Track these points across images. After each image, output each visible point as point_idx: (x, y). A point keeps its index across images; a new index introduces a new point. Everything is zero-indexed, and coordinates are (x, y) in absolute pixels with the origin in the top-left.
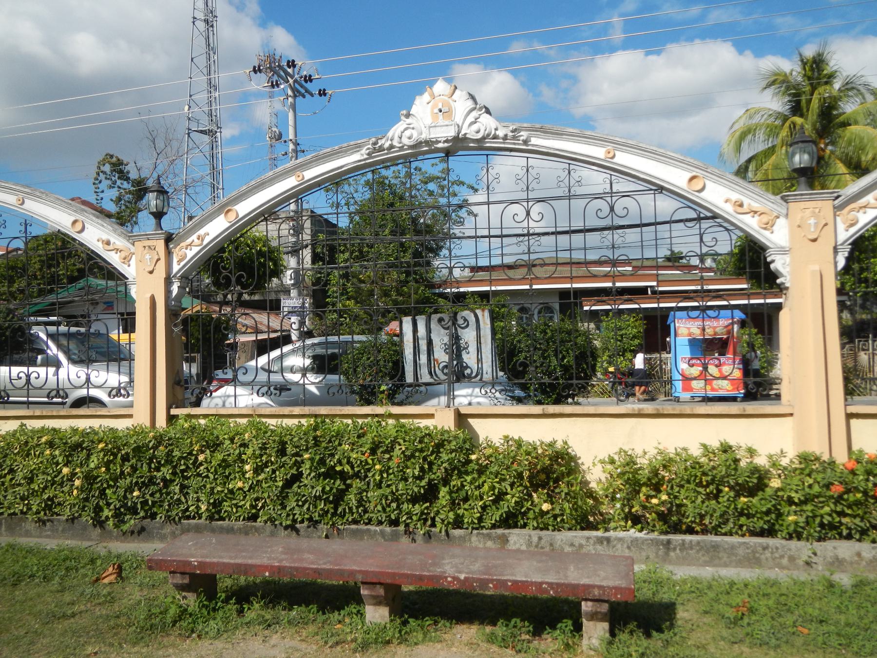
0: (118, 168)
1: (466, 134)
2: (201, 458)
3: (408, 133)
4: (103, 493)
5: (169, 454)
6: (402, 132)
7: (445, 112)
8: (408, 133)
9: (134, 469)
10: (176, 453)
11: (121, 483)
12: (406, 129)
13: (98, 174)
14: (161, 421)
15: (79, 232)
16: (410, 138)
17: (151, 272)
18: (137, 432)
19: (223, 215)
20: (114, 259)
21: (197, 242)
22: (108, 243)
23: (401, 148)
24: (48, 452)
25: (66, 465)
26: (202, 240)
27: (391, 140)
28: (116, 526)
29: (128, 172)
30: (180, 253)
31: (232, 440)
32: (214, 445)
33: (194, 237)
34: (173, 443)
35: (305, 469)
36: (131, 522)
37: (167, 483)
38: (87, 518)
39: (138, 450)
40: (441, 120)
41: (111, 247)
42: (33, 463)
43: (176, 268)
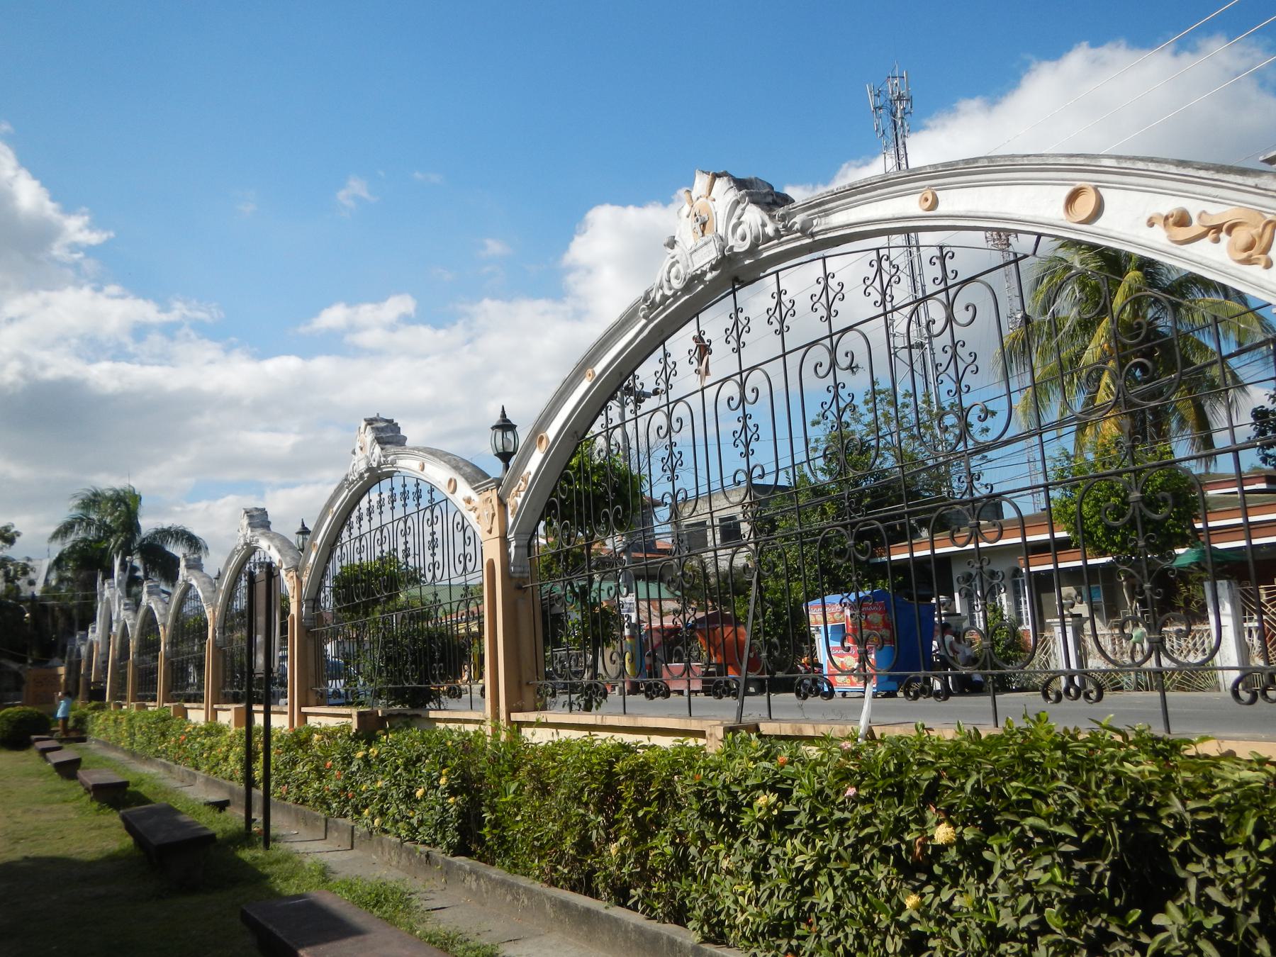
41: (1196, 228)
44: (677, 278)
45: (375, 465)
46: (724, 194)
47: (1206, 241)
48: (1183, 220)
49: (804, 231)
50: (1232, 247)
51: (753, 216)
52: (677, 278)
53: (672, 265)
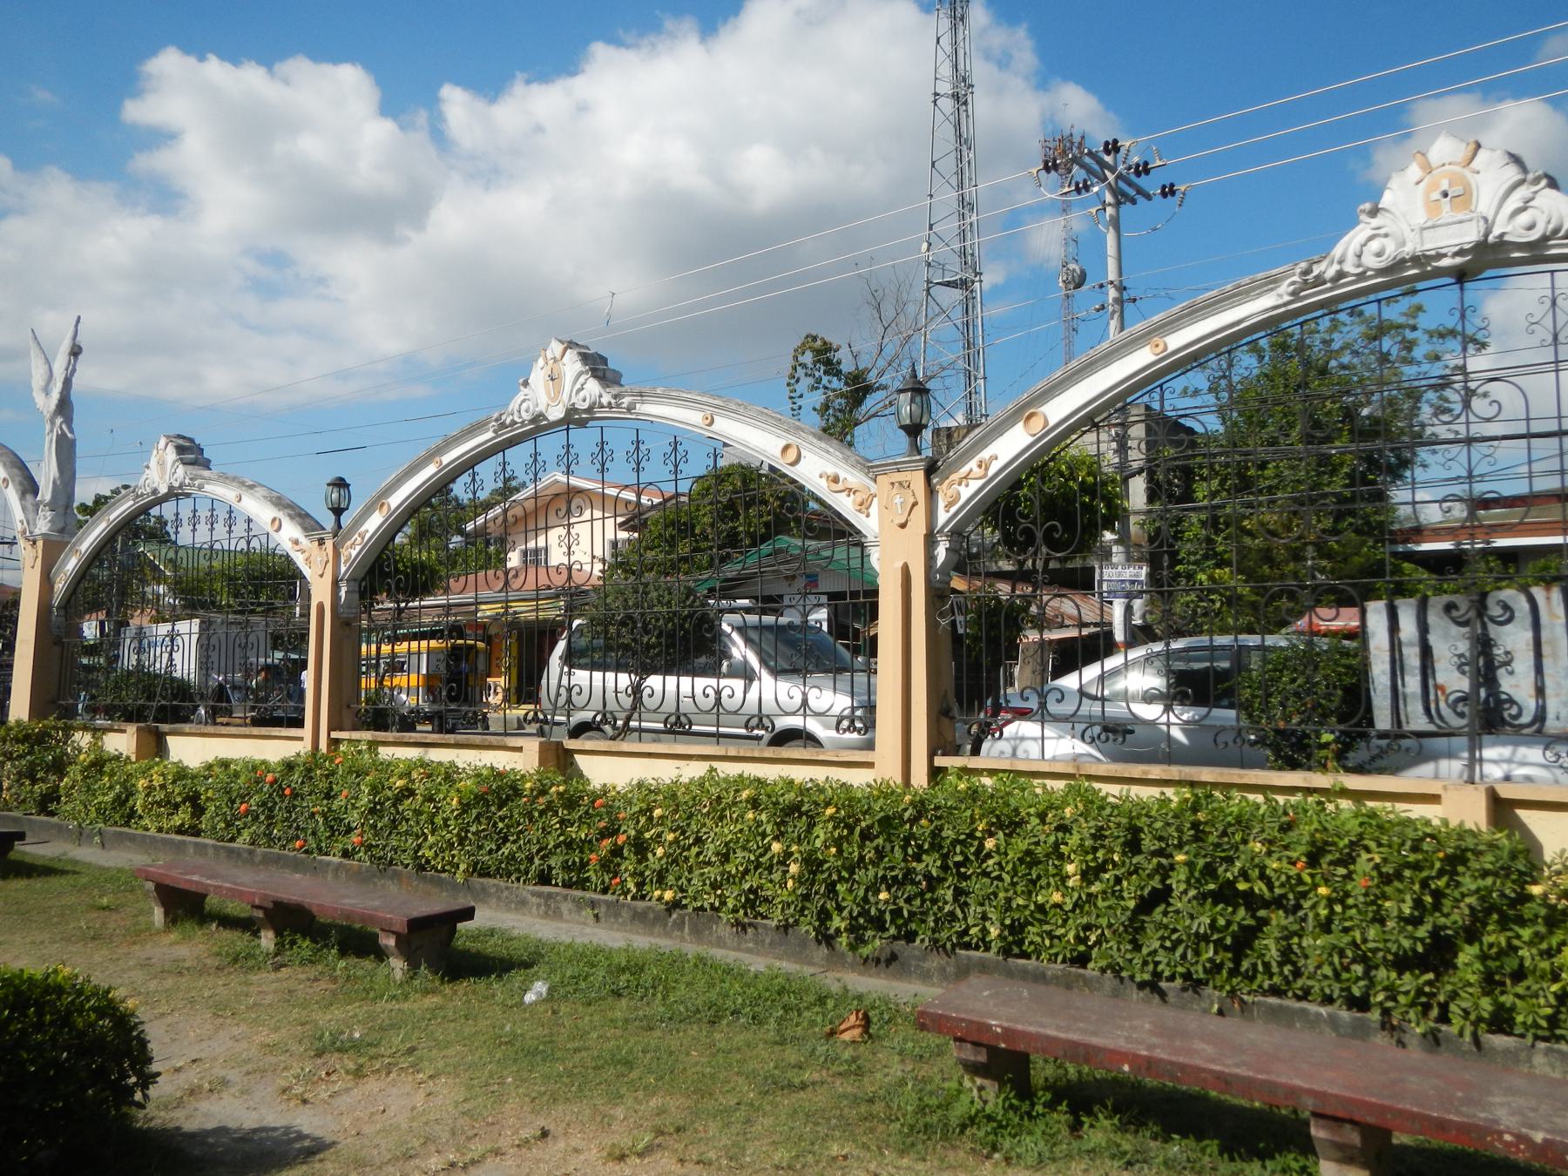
0: (825, 357)
1: (1503, 235)
2: (990, 844)
3: (1375, 245)
4: (831, 889)
5: (936, 834)
6: (1365, 245)
7: (1458, 196)
8: (1375, 245)
9: (880, 853)
10: (948, 833)
11: (859, 875)
12: (1371, 238)
13: (795, 368)
14: (920, 778)
15: (794, 464)
16: (1379, 255)
17: (903, 526)
18: (883, 792)
19: (1021, 423)
20: (845, 505)
21: (977, 471)
22: (836, 480)
23: (1361, 277)
24: (750, 815)
25: (776, 838)
26: (987, 469)
27: (1340, 262)
28: (853, 947)
29: (839, 363)
30: (950, 492)
31: (1042, 817)
32: (1011, 825)
33: (973, 464)
34: (942, 814)
35: (1177, 881)
36: (876, 944)
37: (933, 882)
38: (807, 928)
39: (886, 822)
40: (1447, 211)
41: (840, 486)
42: (728, 830)
43: (942, 517)
44: (527, 411)
45: (176, 484)
46: (572, 365)
47: (844, 494)
48: (836, 480)
49: (629, 409)
50: (854, 501)
51: (593, 387)
52: (527, 411)
53: (524, 401)
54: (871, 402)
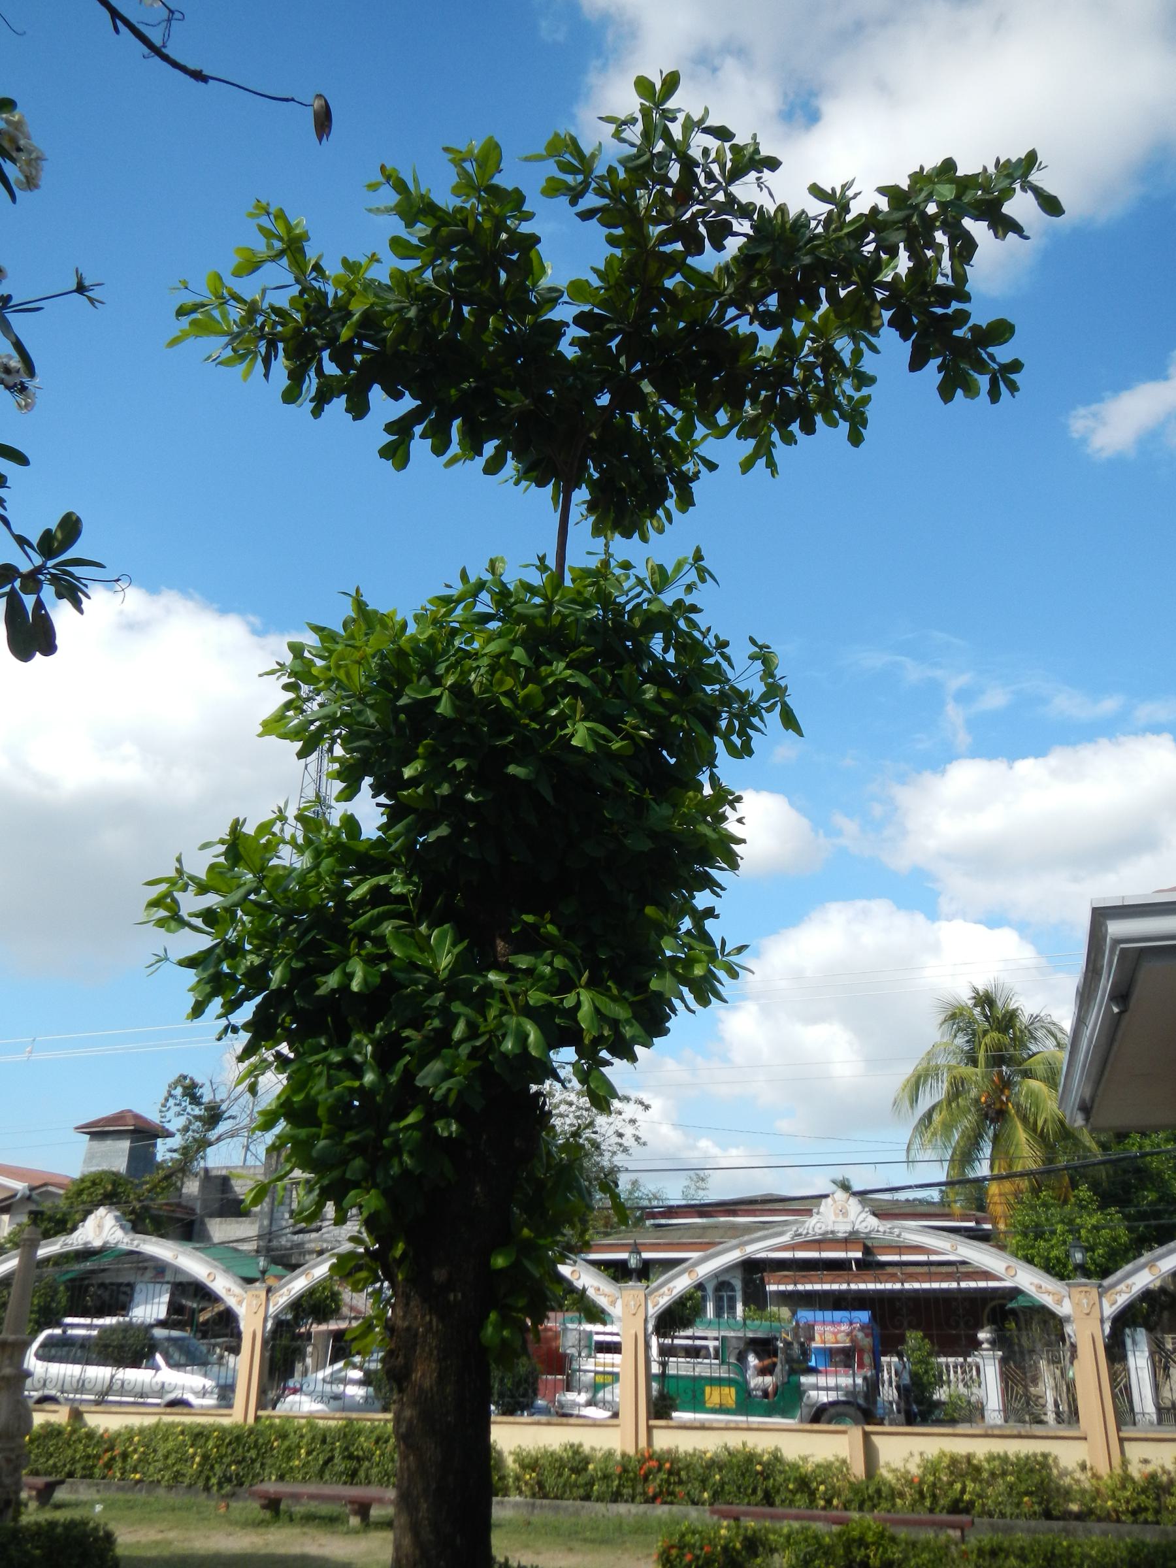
0: (191, 1091)
2: (275, 1444)
4: (212, 1467)
5: (256, 1441)
9: (234, 1451)
10: (261, 1441)
11: (225, 1460)
13: (167, 1100)
14: (251, 1420)
18: (237, 1426)
25: (192, 1446)
28: (218, 1491)
29: (201, 1097)
31: (295, 1432)
32: (283, 1436)
34: (261, 1434)
35: (337, 1453)
36: (228, 1488)
37: (253, 1461)
38: (201, 1484)
39: (238, 1438)
42: (170, 1445)
54: (223, 1127)
